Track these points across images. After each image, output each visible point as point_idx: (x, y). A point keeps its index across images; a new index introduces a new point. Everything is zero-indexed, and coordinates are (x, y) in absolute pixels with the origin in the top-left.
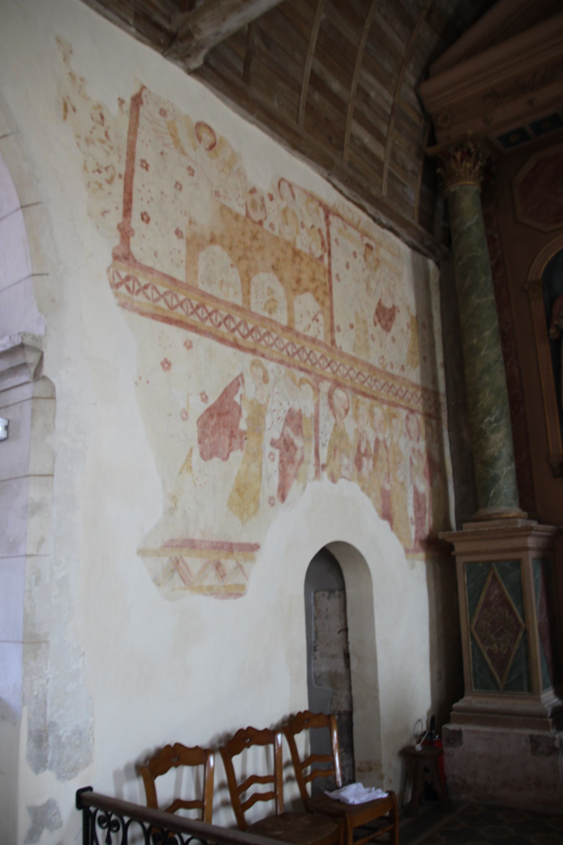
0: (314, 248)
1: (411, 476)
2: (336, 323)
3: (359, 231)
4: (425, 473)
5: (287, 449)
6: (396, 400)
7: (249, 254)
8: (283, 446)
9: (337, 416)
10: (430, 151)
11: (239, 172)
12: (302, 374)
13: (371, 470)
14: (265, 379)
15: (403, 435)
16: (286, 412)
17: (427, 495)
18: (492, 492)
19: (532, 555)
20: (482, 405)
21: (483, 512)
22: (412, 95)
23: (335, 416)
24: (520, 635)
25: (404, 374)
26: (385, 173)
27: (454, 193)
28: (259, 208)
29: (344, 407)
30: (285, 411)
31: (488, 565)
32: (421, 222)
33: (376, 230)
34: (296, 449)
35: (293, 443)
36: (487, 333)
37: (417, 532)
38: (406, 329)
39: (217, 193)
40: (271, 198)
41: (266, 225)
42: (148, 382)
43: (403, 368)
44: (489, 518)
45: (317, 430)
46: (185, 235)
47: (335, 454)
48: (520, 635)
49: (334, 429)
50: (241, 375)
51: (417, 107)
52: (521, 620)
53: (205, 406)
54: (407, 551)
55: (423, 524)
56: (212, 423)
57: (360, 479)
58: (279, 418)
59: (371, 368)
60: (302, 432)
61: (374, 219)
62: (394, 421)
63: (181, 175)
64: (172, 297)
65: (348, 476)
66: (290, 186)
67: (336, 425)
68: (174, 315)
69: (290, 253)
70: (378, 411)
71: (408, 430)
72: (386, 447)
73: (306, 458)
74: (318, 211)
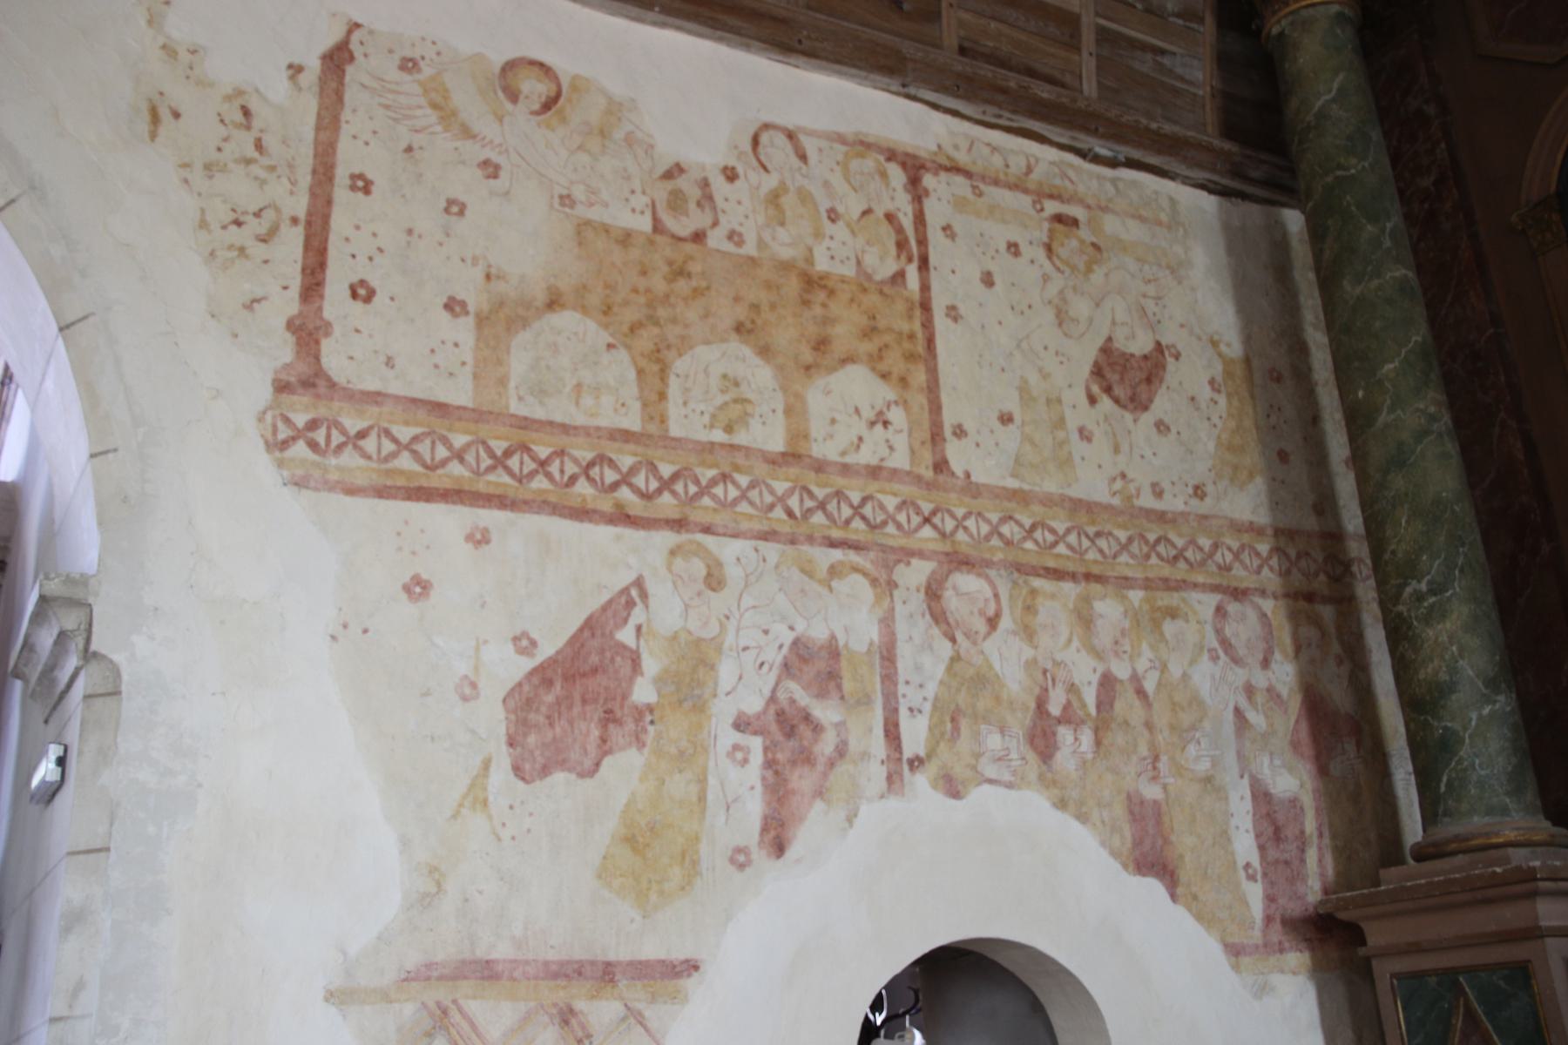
0: (870, 260)
1: (1240, 756)
2: (949, 418)
3: (1026, 191)
4: (1295, 745)
5: (790, 732)
6: (1180, 571)
7: (662, 313)
8: (774, 728)
9: (959, 637)
11: (630, 141)
12: (837, 555)
13: (1090, 756)
14: (714, 580)
15: (1206, 656)
16: (785, 650)
17: (1308, 801)
18: (1445, 779)
20: (1393, 552)
23: (953, 640)
25: (1204, 507)
26: (1088, 38)
27: (1281, 34)
28: (692, 206)
29: (982, 613)
30: (781, 647)
31: (1449, 977)
32: (1229, 130)
33: (1089, 178)
34: (817, 728)
35: (807, 718)
37: (1270, 899)
38: (1206, 393)
39: (567, 200)
40: (731, 175)
41: (716, 239)
42: (365, 631)
43: (1199, 492)
45: (889, 678)
46: (471, 308)
47: (956, 729)
49: (949, 669)
50: (639, 583)
53: (527, 664)
54: (1235, 951)
55: (1297, 877)
56: (550, 698)
57: (1048, 781)
58: (762, 664)
59: (1078, 506)
60: (839, 687)
61: (1082, 154)
62: (1169, 627)
63: (465, 182)
64: (433, 443)
65: (1007, 777)
66: (791, 135)
67: (956, 658)
68: (436, 480)
69: (793, 286)
70: (1109, 610)
71: (1225, 644)
72: (1141, 692)
73: (854, 746)
74: (883, 175)
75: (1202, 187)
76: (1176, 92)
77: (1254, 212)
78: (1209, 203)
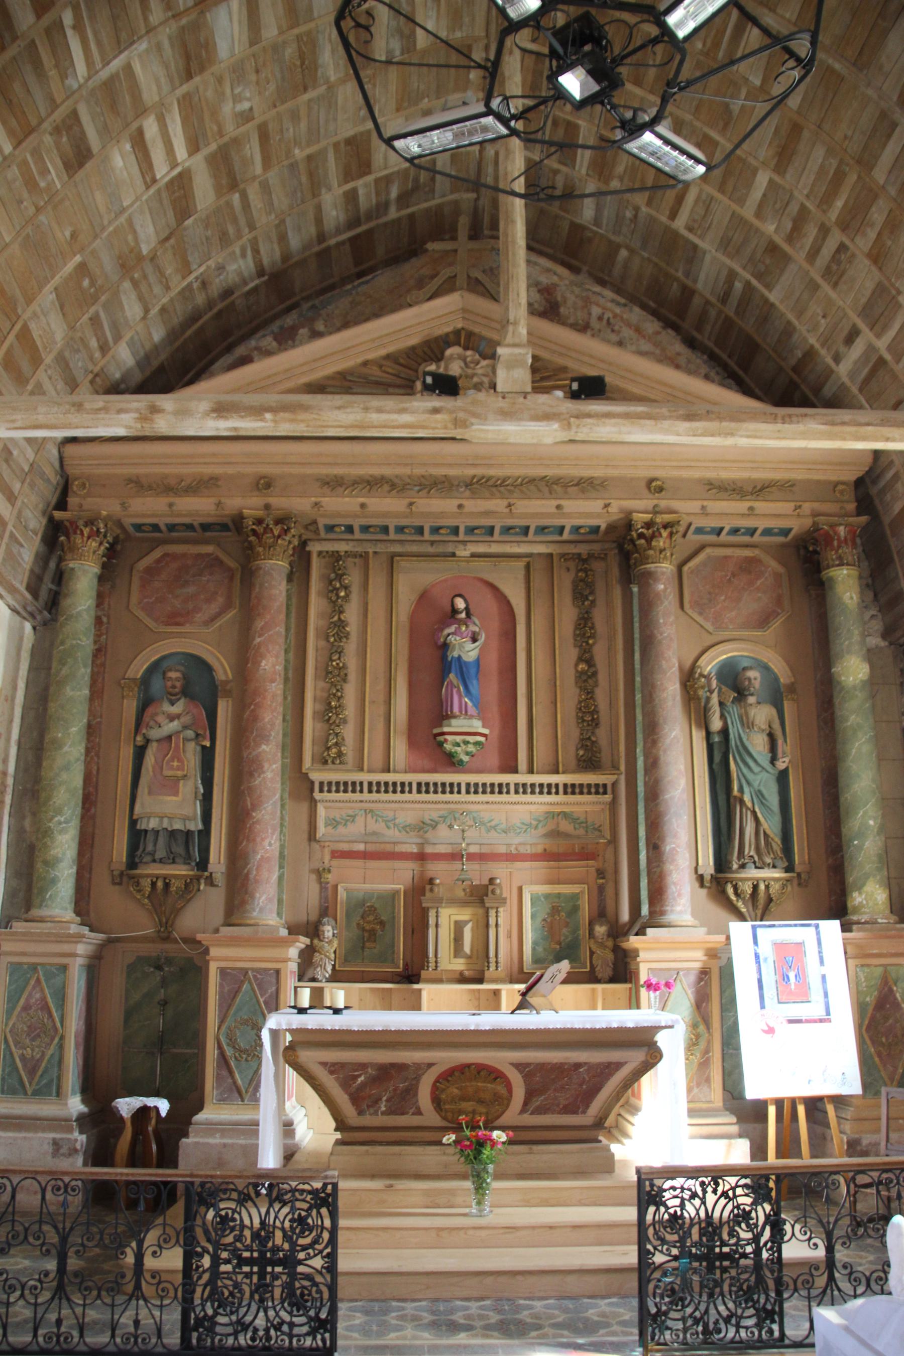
10: (58, 515)
19: (80, 961)
21: (35, 912)
22: (55, 452)
24: (56, 1040)
26: (7, 534)
27: (73, 569)
31: (34, 967)
32: (28, 588)
36: (74, 729)
44: (41, 920)
48: (56, 1040)
51: (57, 464)
52: (58, 1025)
75: (9, 606)
76: (20, 564)
77: (18, 618)
78: (7, 612)
